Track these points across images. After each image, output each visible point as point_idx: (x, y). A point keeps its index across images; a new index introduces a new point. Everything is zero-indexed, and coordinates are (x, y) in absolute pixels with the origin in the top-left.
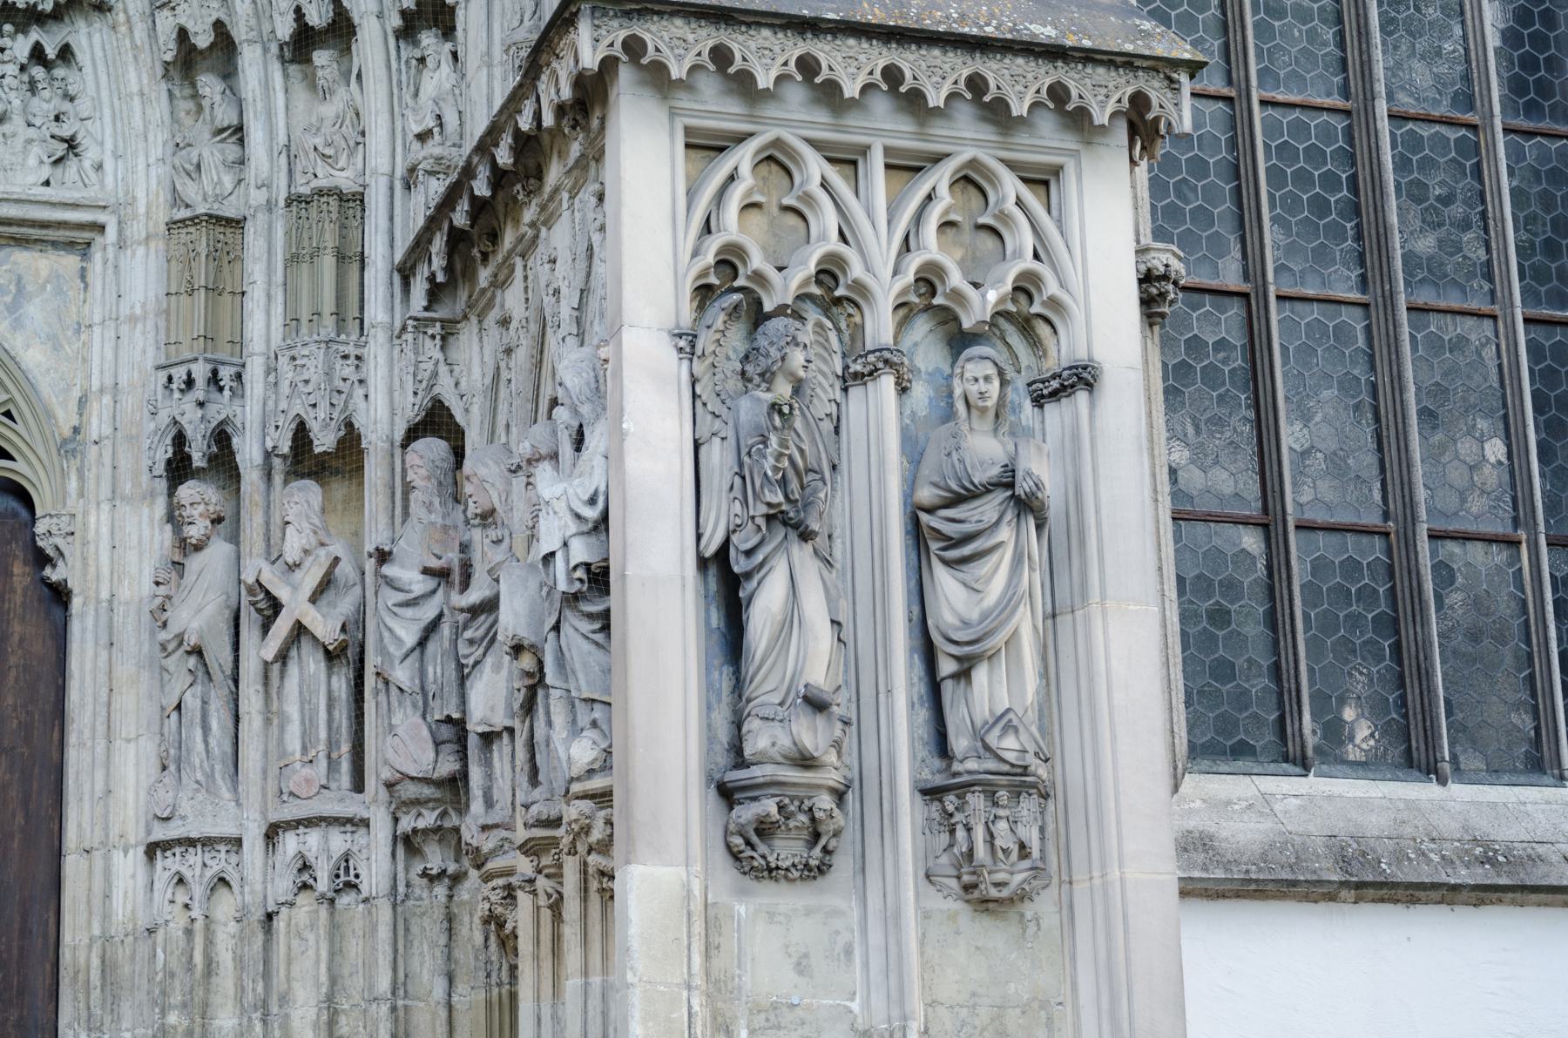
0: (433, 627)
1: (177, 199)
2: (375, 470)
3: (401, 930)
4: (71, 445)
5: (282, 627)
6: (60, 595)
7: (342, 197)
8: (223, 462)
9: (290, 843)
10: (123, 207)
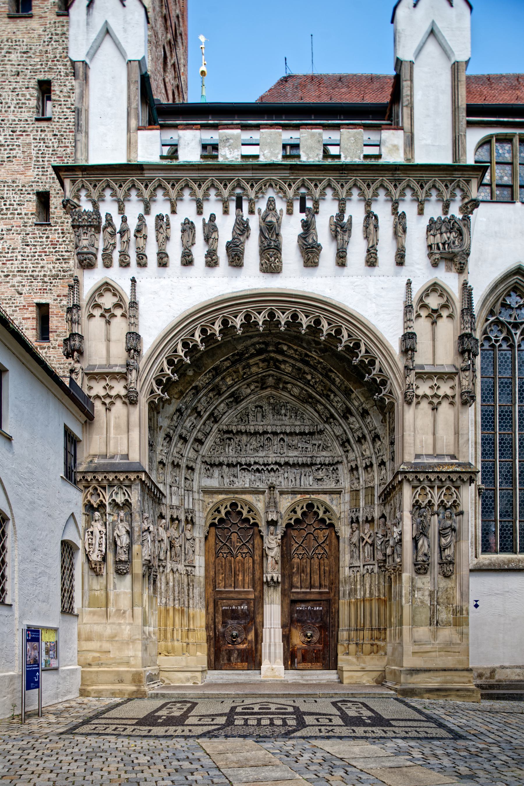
0: (382, 542)
1: (351, 488)
2: (376, 522)
3: (379, 577)
4: (339, 518)
5: (365, 542)
6: (338, 538)
7: (371, 487)
8: (358, 521)
9: (366, 567)
10: (344, 488)
